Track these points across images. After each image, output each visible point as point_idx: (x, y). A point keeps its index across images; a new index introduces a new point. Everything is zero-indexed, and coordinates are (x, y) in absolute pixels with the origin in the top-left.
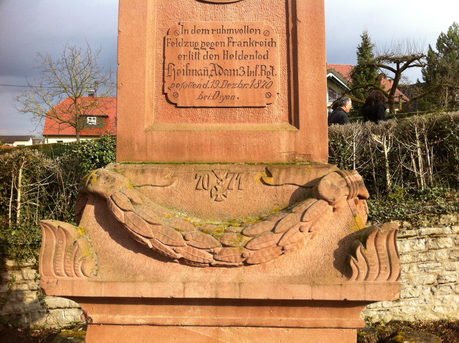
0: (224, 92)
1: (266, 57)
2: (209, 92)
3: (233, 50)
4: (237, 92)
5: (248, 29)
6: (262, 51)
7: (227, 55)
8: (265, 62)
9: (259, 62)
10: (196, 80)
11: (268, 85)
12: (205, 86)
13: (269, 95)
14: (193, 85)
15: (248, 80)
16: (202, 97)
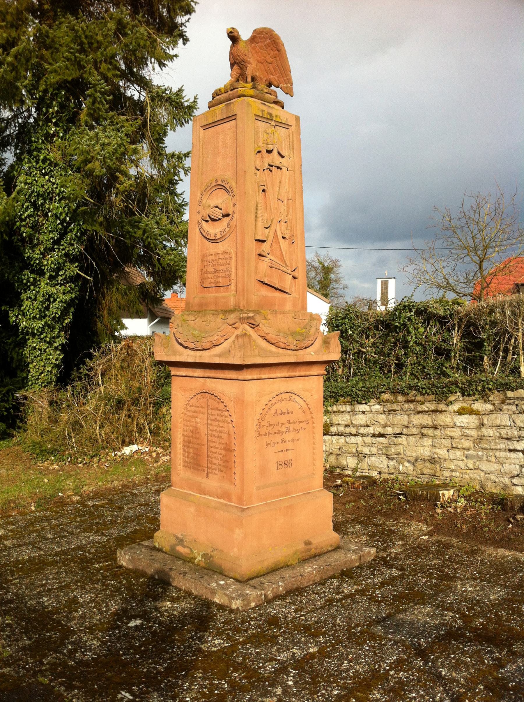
0: (217, 280)
1: (229, 264)
2: (213, 281)
3: (221, 262)
4: (220, 280)
5: (225, 253)
6: (228, 261)
7: (218, 265)
8: (229, 266)
9: (227, 266)
10: (209, 276)
11: (229, 276)
12: (211, 278)
13: (230, 280)
14: (208, 278)
15: (224, 274)
16: (211, 283)
